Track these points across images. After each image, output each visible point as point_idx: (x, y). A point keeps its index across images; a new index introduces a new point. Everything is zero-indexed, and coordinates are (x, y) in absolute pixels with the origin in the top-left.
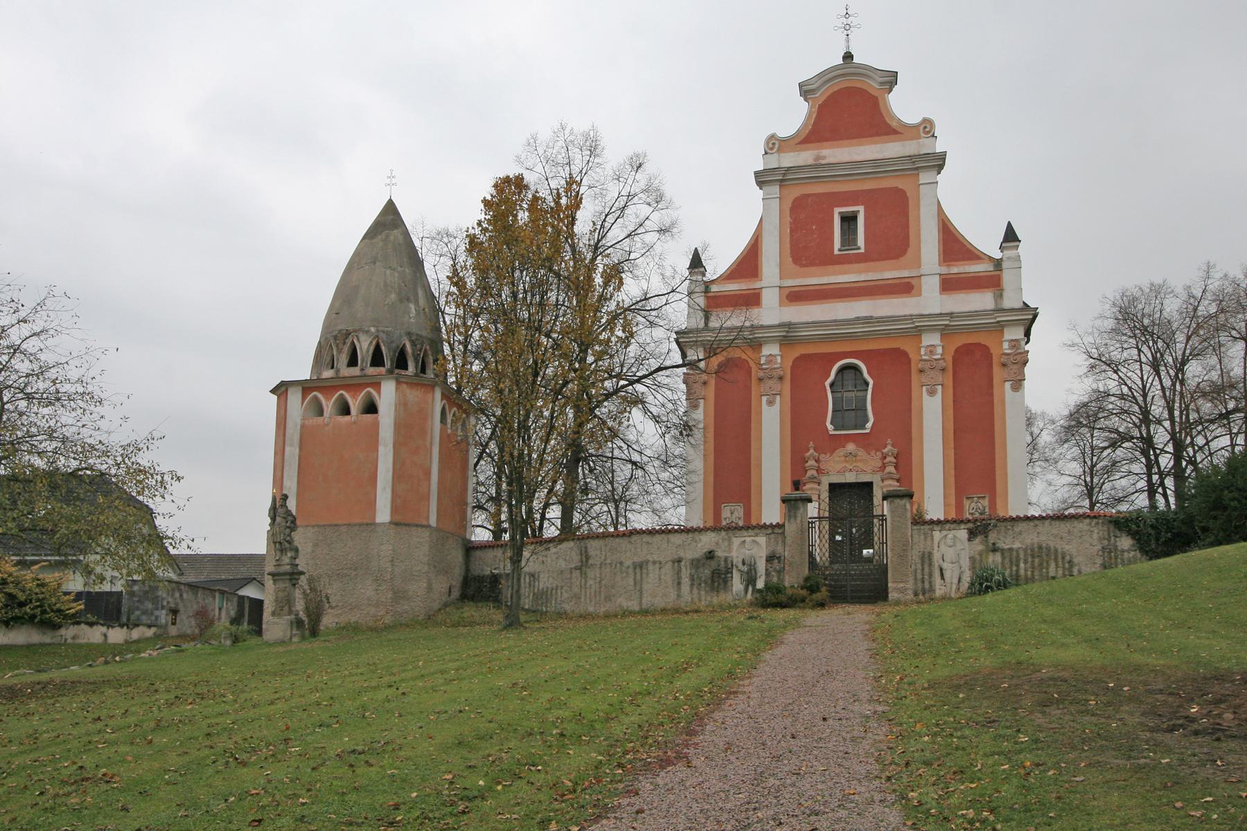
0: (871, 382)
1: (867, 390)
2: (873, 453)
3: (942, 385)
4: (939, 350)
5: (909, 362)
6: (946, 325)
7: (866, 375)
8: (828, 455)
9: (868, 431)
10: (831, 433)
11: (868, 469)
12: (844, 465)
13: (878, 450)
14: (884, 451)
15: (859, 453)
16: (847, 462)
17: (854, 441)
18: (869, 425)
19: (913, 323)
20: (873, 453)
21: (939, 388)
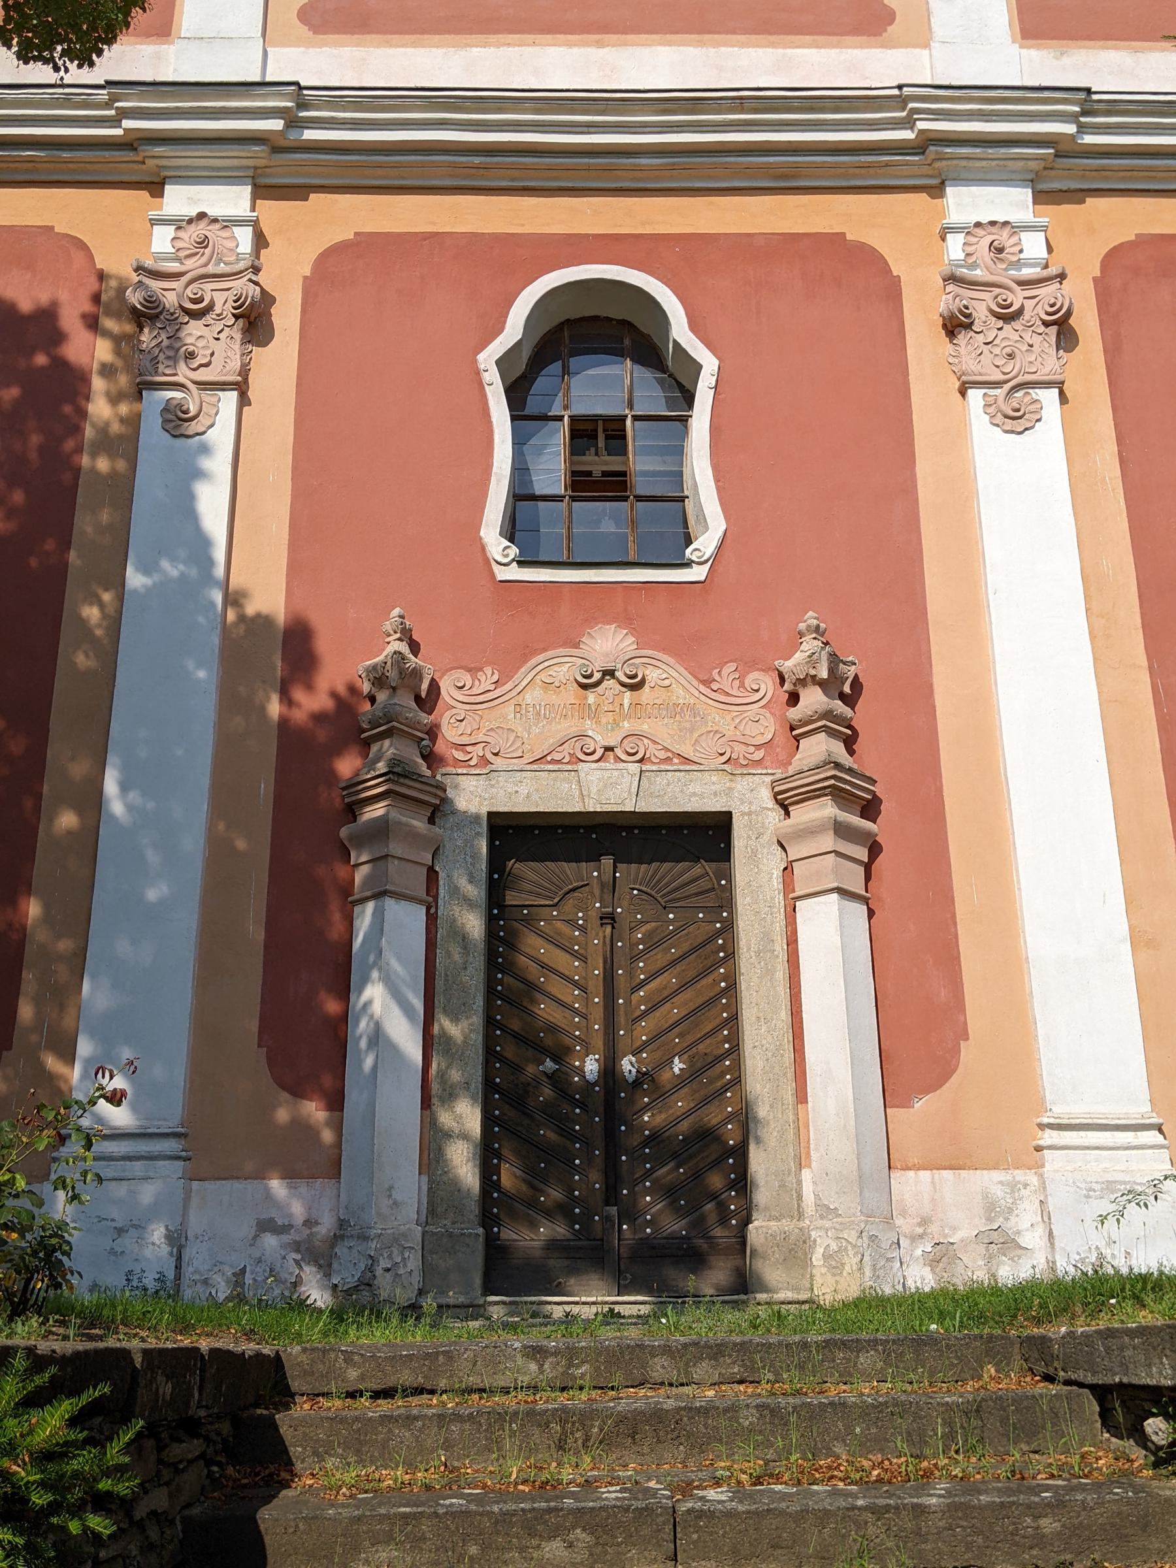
0: (709, 363)
1: (684, 420)
2: (726, 676)
3: (1060, 385)
4: (1033, 246)
5: (892, 291)
6: (1062, 148)
7: (680, 331)
8: (487, 677)
9: (697, 573)
10: (502, 574)
11: (705, 750)
12: (569, 727)
13: (748, 664)
14: (787, 665)
15: (653, 675)
16: (584, 710)
17: (626, 620)
18: (705, 544)
19: (908, 123)
20: (726, 676)
21: (1050, 397)
